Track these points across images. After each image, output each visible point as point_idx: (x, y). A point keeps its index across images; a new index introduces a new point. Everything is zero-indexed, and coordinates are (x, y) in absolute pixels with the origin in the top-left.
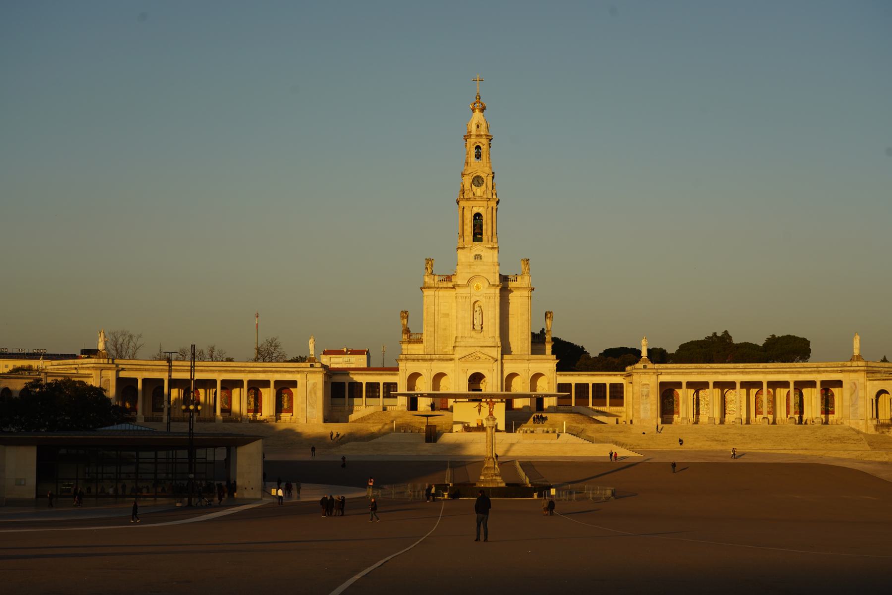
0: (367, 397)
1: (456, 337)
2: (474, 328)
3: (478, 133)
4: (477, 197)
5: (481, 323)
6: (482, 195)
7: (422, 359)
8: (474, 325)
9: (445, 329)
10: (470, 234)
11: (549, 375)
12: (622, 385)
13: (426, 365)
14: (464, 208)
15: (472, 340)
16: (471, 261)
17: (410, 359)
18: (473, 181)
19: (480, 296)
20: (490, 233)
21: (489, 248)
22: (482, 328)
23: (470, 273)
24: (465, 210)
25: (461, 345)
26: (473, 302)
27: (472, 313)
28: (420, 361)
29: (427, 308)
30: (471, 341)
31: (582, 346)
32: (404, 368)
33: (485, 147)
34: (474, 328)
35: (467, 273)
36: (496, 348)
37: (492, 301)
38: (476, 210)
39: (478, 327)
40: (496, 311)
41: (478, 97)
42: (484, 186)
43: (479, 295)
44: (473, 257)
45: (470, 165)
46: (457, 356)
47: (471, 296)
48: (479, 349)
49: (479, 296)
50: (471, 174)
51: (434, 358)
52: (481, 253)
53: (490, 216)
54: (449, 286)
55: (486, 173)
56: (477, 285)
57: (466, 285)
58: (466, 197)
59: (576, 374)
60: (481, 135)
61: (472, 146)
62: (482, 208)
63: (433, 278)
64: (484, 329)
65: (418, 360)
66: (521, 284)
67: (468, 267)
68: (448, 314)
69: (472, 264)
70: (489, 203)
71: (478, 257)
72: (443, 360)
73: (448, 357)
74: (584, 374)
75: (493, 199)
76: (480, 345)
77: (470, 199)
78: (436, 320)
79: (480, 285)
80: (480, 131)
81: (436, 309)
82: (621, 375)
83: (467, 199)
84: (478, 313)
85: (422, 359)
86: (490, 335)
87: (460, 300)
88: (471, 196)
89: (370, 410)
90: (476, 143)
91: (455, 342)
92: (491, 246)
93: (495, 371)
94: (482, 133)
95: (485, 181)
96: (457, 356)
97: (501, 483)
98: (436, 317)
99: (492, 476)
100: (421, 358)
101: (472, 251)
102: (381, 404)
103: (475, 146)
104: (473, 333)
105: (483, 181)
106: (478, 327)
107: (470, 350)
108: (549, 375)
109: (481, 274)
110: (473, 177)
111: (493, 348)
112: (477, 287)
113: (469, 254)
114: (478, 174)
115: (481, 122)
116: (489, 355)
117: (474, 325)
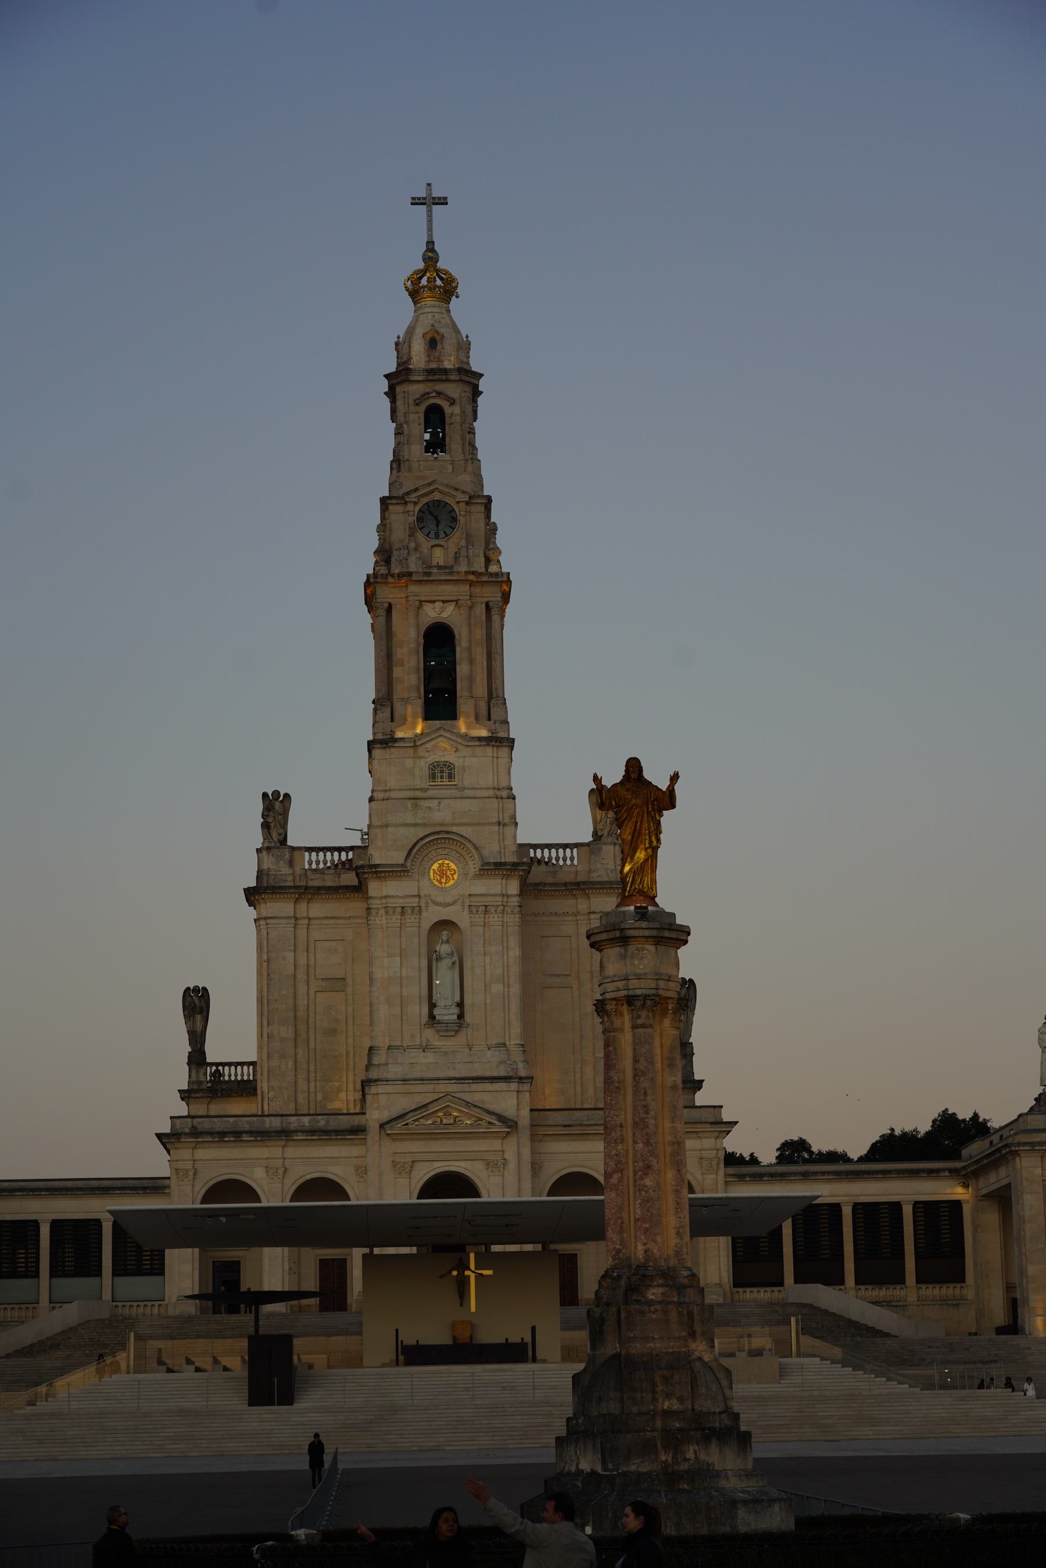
0: (54, 1273)
1: (371, 1049)
2: (432, 1017)
3: (434, 365)
4: (435, 571)
5: (457, 999)
6: (451, 562)
7: (250, 1133)
8: (432, 1006)
9: (333, 1032)
10: (414, 694)
11: (699, 1177)
12: (956, 1206)
13: (271, 1151)
15: (430, 1058)
16: (418, 783)
17: (211, 1133)
18: (420, 519)
19: (454, 903)
20: (481, 690)
21: (480, 739)
22: (461, 1016)
23: (415, 825)
24: (394, 613)
25: (390, 1076)
26: (426, 925)
27: (424, 963)
28: (245, 1138)
29: (268, 961)
30: (424, 1063)
31: (752, 1155)
32: (189, 1165)
33: (457, 409)
34: (432, 1017)
35: (406, 825)
36: (514, 1086)
37: (495, 919)
38: (432, 614)
39: (446, 1013)
40: (511, 953)
41: (431, 256)
42: (456, 540)
43: (449, 900)
44: (426, 772)
45: (410, 470)
46: (375, 1116)
47: (423, 905)
48: (452, 1087)
49: (447, 905)
50: (413, 497)
51: (292, 1127)
52: (451, 757)
53: (480, 634)
54: (342, 884)
55: (464, 492)
56: (440, 865)
57: (402, 865)
58: (396, 570)
59: (795, 1174)
60: (446, 371)
61: (413, 408)
62: (450, 608)
63: (287, 856)
64: (468, 1018)
65: (237, 1134)
66: (589, 872)
67: (409, 803)
68: (344, 979)
69: (418, 794)
70: (477, 590)
71: (442, 771)
72: (326, 1132)
73: (344, 1122)
74: (824, 1173)
75: (491, 575)
76: (458, 1075)
77: (410, 574)
78: (302, 1002)
79: (453, 866)
80: (440, 361)
81: (302, 961)
82: (951, 1171)
83: (401, 576)
84: (446, 962)
85: (250, 1133)
86: (494, 1040)
87: (379, 920)
88: (414, 565)
89: (71, 1314)
90: (425, 395)
91: (369, 1066)
92: (484, 733)
93: (512, 1165)
94: (447, 365)
95: (462, 520)
96: (375, 1116)
97: (756, 1502)
98: (302, 989)
99: (674, 1441)
100: (247, 1127)
101: (421, 751)
102: (107, 1295)
103: (423, 408)
104: (429, 1033)
105: (454, 519)
106: (446, 1013)
107: (423, 1094)
108: (699, 1177)
109: (454, 829)
110: (417, 508)
111: (502, 1086)
112: (442, 873)
113: (409, 763)
114: (437, 496)
115: (442, 331)
116: (488, 1106)
117: (432, 1006)
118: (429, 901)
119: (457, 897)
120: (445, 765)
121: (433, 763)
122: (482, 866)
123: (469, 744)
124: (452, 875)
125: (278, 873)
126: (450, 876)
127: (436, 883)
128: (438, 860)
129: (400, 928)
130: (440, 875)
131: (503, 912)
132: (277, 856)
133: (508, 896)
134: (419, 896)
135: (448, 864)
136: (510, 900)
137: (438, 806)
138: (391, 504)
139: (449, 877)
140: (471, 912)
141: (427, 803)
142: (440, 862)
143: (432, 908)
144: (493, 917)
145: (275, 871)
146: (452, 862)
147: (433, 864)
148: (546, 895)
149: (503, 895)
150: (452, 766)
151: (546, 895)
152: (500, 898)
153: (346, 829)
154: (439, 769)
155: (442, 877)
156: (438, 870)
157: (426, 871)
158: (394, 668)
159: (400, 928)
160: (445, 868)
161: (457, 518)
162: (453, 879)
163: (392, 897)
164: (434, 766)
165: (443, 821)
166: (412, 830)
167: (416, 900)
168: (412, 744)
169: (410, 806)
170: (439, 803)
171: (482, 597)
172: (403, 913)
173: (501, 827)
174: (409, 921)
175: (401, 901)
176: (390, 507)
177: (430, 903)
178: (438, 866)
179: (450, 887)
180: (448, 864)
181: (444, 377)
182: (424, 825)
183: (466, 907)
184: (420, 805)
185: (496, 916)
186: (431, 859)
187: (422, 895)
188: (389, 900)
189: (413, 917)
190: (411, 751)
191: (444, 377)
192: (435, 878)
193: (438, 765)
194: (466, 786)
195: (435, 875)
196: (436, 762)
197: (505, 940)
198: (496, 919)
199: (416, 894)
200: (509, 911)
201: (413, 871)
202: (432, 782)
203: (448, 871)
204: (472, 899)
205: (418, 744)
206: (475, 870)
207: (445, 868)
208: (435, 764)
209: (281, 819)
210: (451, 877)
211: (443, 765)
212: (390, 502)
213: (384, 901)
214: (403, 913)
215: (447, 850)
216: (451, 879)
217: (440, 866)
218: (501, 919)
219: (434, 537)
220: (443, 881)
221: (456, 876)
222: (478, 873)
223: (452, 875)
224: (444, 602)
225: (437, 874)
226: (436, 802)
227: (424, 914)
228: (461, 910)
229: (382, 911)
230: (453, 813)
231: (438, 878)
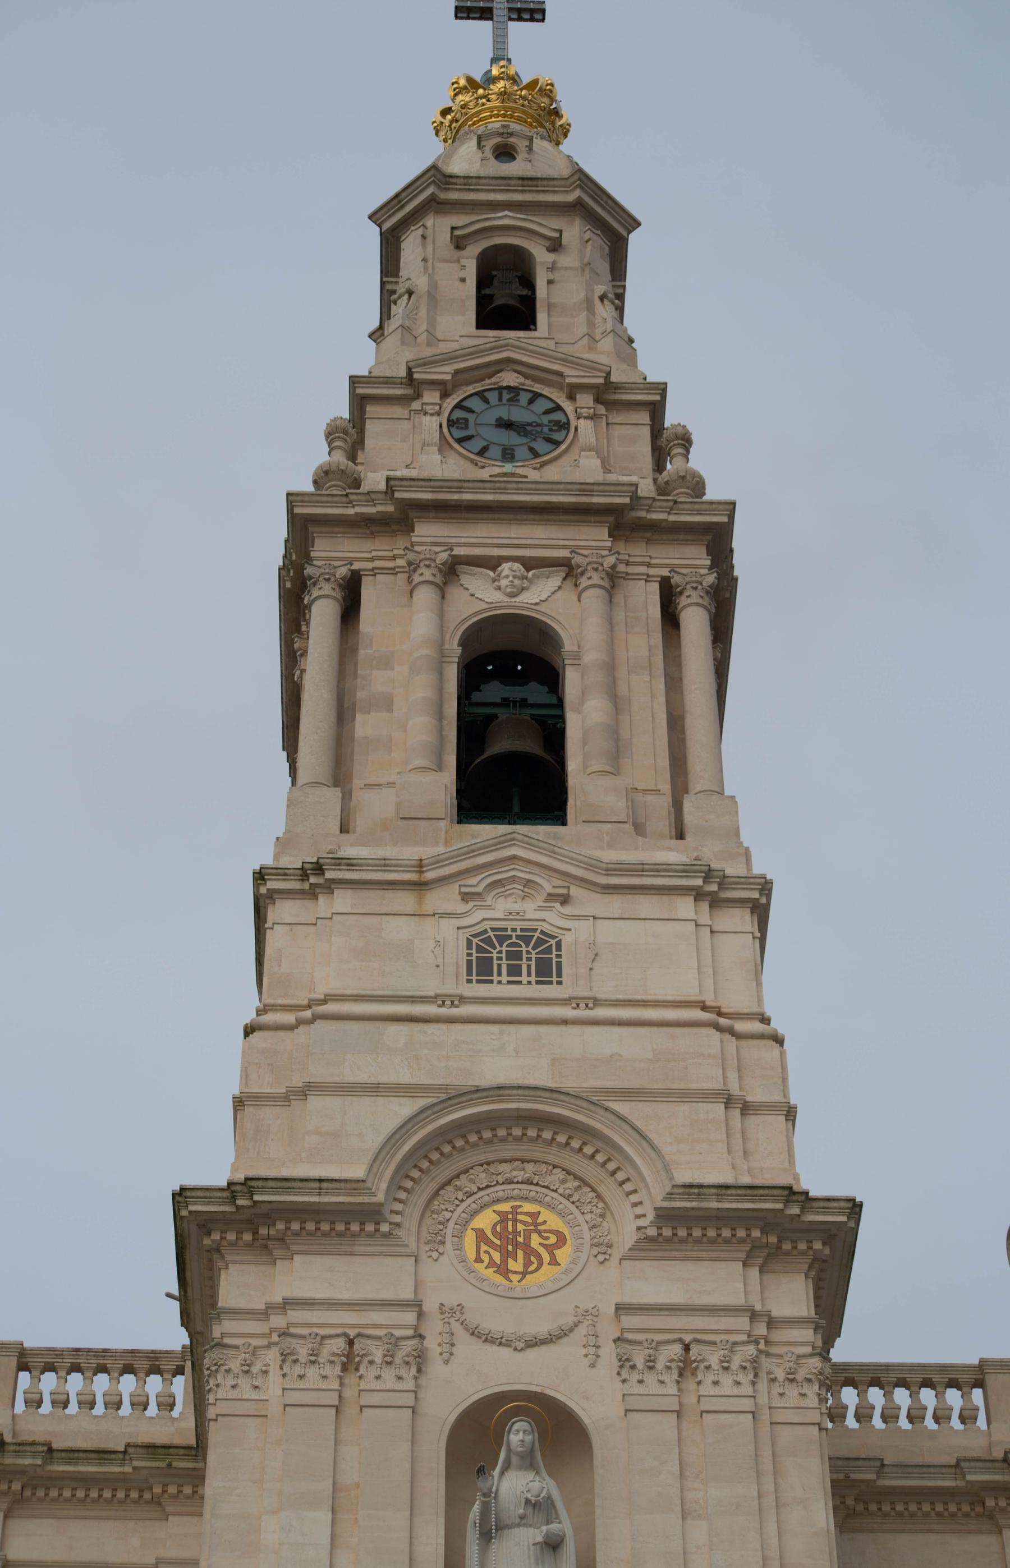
43: (543, 1329)
56: (503, 1218)
118: (456, 1326)
119: (571, 1320)
120: (527, 940)
121: (485, 931)
122: (669, 1196)
124: (550, 1249)
126: (541, 1250)
128: (498, 1201)
129: (338, 1410)
130: (500, 1249)
131: (754, 1367)
133: (772, 1323)
134: (417, 1305)
136: (778, 1335)
140: (625, 1363)
142: (505, 1207)
143: (467, 1347)
144: (716, 1383)
146: (550, 1207)
148: (885, 1515)
149: (754, 1316)
150: (553, 942)
151: (885, 1515)
152: (743, 1322)
154: (504, 949)
155: (506, 1255)
156: (494, 1232)
157: (449, 1231)
158: (359, 717)
159: (338, 1410)
160: (520, 1227)
161: (568, 423)
162: (554, 1262)
163: (310, 1304)
164: (488, 941)
167: (409, 1317)
171: (649, 565)
172: (349, 1362)
173: (736, 1113)
174: (374, 1385)
177: (462, 1336)
178: (498, 1218)
183: (609, 1352)
185: (726, 1380)
186: (470, 1195)
187: (430, 1306)
188: (295, 1315)
189: (389, 1375)
192: (485, 1258)
193: (501, 940)
194: (600, 996)
195: (484, 1247)
196: (493, 929)
197: (767, 1465)
199: (408, 1295)
200: (781, 1375)
201: (397, 1219)
204: (630, 1321)
205: (430, 875)
206: (641, 1222)
208: (491, 934)
210: (546, 1257)
211: (518, 936)
213: (278, 1321)
214: (349, 1362)
215: (530, 1167)
216: (546, 1257)
218: (748, 1390)
221: (563, 1255)
222: (652, 1232)
223: (550, 1249)
224: (529, 564)
227: (436, 1368)
228: (586, 1362)
229: (272, 1357)
231: (497, 1256)
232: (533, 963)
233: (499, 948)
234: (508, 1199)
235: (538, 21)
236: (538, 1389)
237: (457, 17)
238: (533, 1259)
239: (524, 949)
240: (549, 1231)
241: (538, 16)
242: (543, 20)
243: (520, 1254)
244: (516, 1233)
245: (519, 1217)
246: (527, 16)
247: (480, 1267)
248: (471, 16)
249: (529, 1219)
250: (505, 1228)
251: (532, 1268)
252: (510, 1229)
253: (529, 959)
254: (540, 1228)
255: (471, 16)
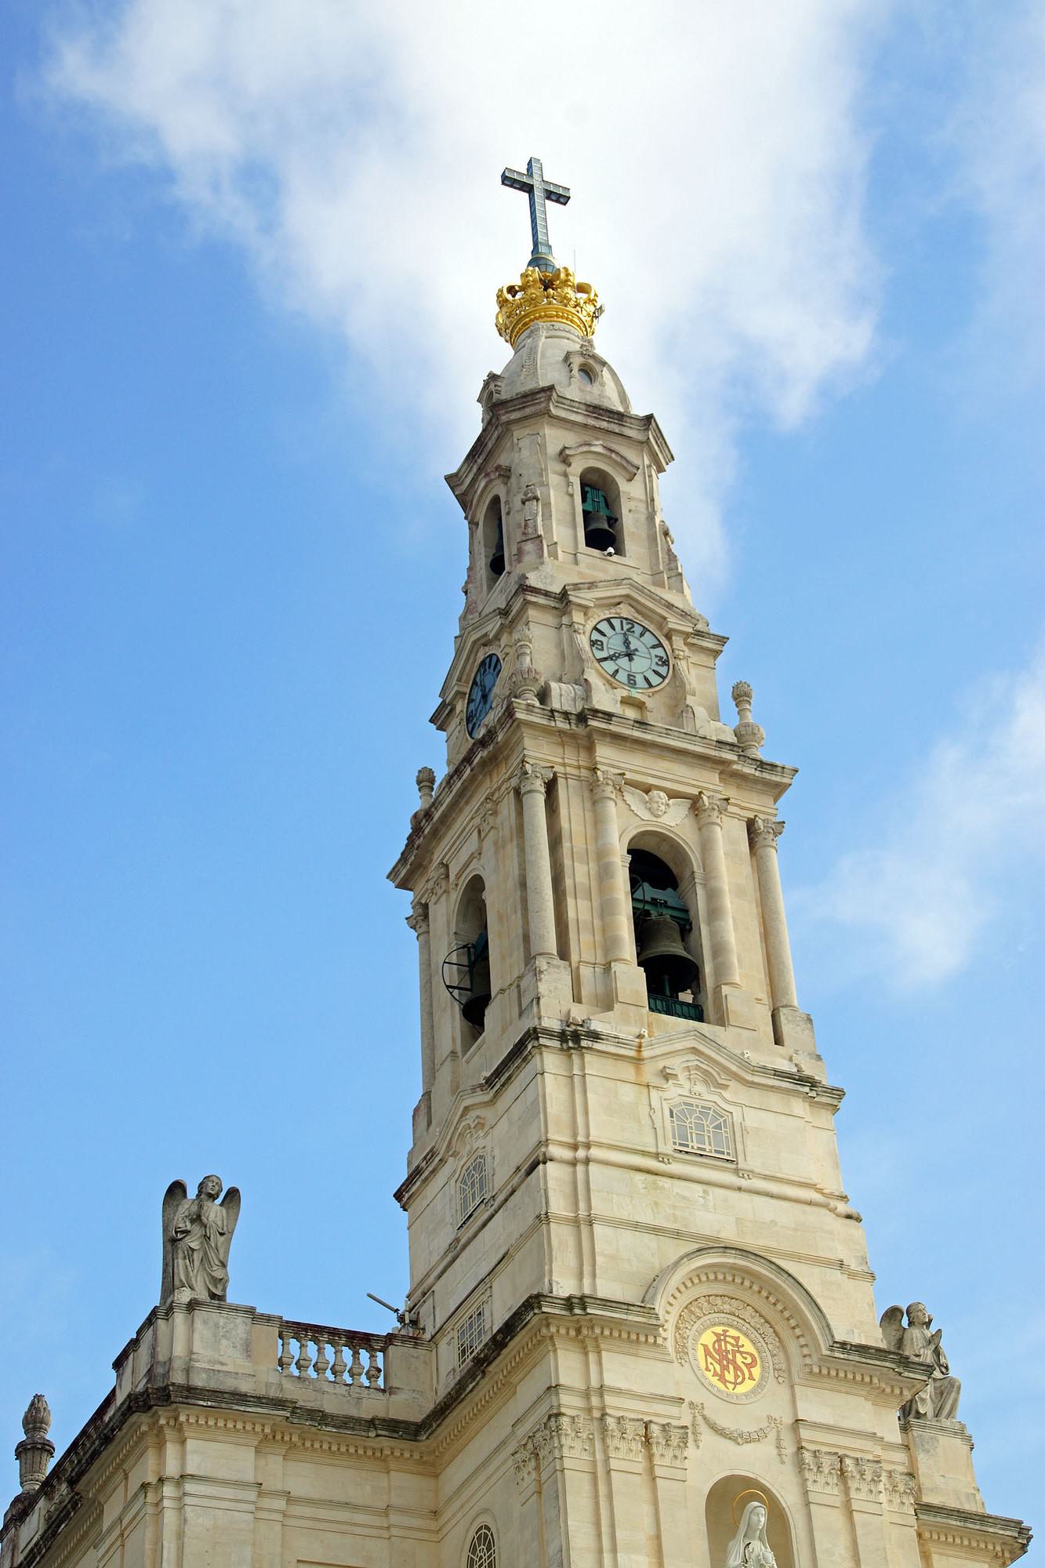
14: (551, 787)
21: (779, 1074)
23: (656, 1230)
35: (636, 1226)
79: (748, 1347)
118: (700, 1420)
123: (756, 1079)
125: (217, 1367)
127: (715, 1380)
130: (720, 1362)
132: (217, 1325)
135: (737, 1339)
137: (704, 1198)
138: (535, 604)
139: (742, 1371)
141: (679, 1187)
142: (719, 1329)
143: (707, 1436)
145: (209, 1362)
146: (746, 1335)
147: (700, 1334)
153: (369, 1296)
155: (725, 1368)
160: (729, 1347)
162: (751, 1378)
165: (719, 1232)
166: (650, 1240)
168: (632, 1053)
169: (641, 1185)
170: (704, 1191)
175: (641, 1406)
176: (532, 613)
177: (703, 1428)
178: (715, 1338)
179: (746, 1395)
180: (737, 1339)
181: (617, 429)
182: (677, 1235)
184: (663, 1188)
190: (628, 1071)
191: (617, 429)
192: (711, 1367)
193: (691, 1112)
195: (710, 1360)
198: (863, 1495)
202: (680, 1144)
203: (738, 1355)
207: (729, 1347)
209: (222, 1243)
212: (533, 599)
217: (719, 1341)
219: (626, 682)
220: (729, 1377)
221: (756, 1371)
225: (713, 1357)
226: (699, 1188)
230: (737, 1219)
232: (711, 1135)
233: (689, 1120)
234: (720, 1324)
235: (562, 203)
236: (751, 1475)
237: (503, 183)
238: (739, 1373)
239: (704, 1122)
240: (746, 1353)
241: (562, 200)
242: (565, 204)
243: (731, 1367)
244: (727, 1352)
245: (728, 1339)
246: (554, 198)
247: (709, 1375)
248: (514, 185)
249: (733, 1342)
250: (720, 1346)
251: (739, 1381)
252: (723, 1348)
253: (709, 1131)
254: (741, 1349)
255: (514, 185)
